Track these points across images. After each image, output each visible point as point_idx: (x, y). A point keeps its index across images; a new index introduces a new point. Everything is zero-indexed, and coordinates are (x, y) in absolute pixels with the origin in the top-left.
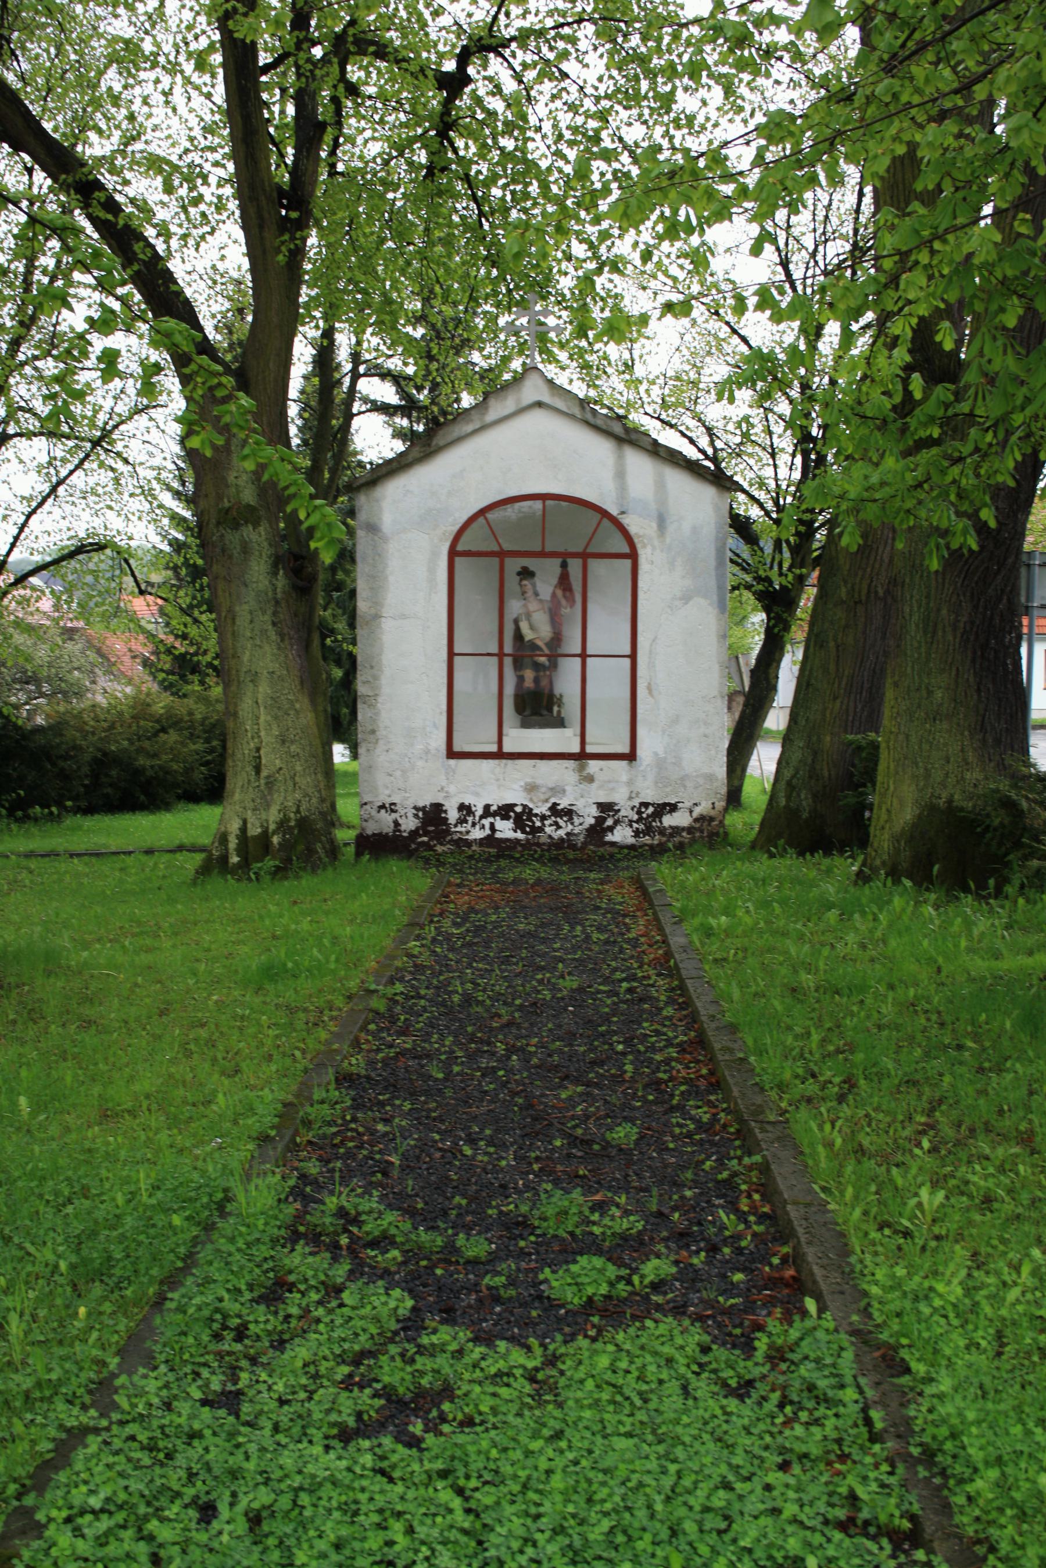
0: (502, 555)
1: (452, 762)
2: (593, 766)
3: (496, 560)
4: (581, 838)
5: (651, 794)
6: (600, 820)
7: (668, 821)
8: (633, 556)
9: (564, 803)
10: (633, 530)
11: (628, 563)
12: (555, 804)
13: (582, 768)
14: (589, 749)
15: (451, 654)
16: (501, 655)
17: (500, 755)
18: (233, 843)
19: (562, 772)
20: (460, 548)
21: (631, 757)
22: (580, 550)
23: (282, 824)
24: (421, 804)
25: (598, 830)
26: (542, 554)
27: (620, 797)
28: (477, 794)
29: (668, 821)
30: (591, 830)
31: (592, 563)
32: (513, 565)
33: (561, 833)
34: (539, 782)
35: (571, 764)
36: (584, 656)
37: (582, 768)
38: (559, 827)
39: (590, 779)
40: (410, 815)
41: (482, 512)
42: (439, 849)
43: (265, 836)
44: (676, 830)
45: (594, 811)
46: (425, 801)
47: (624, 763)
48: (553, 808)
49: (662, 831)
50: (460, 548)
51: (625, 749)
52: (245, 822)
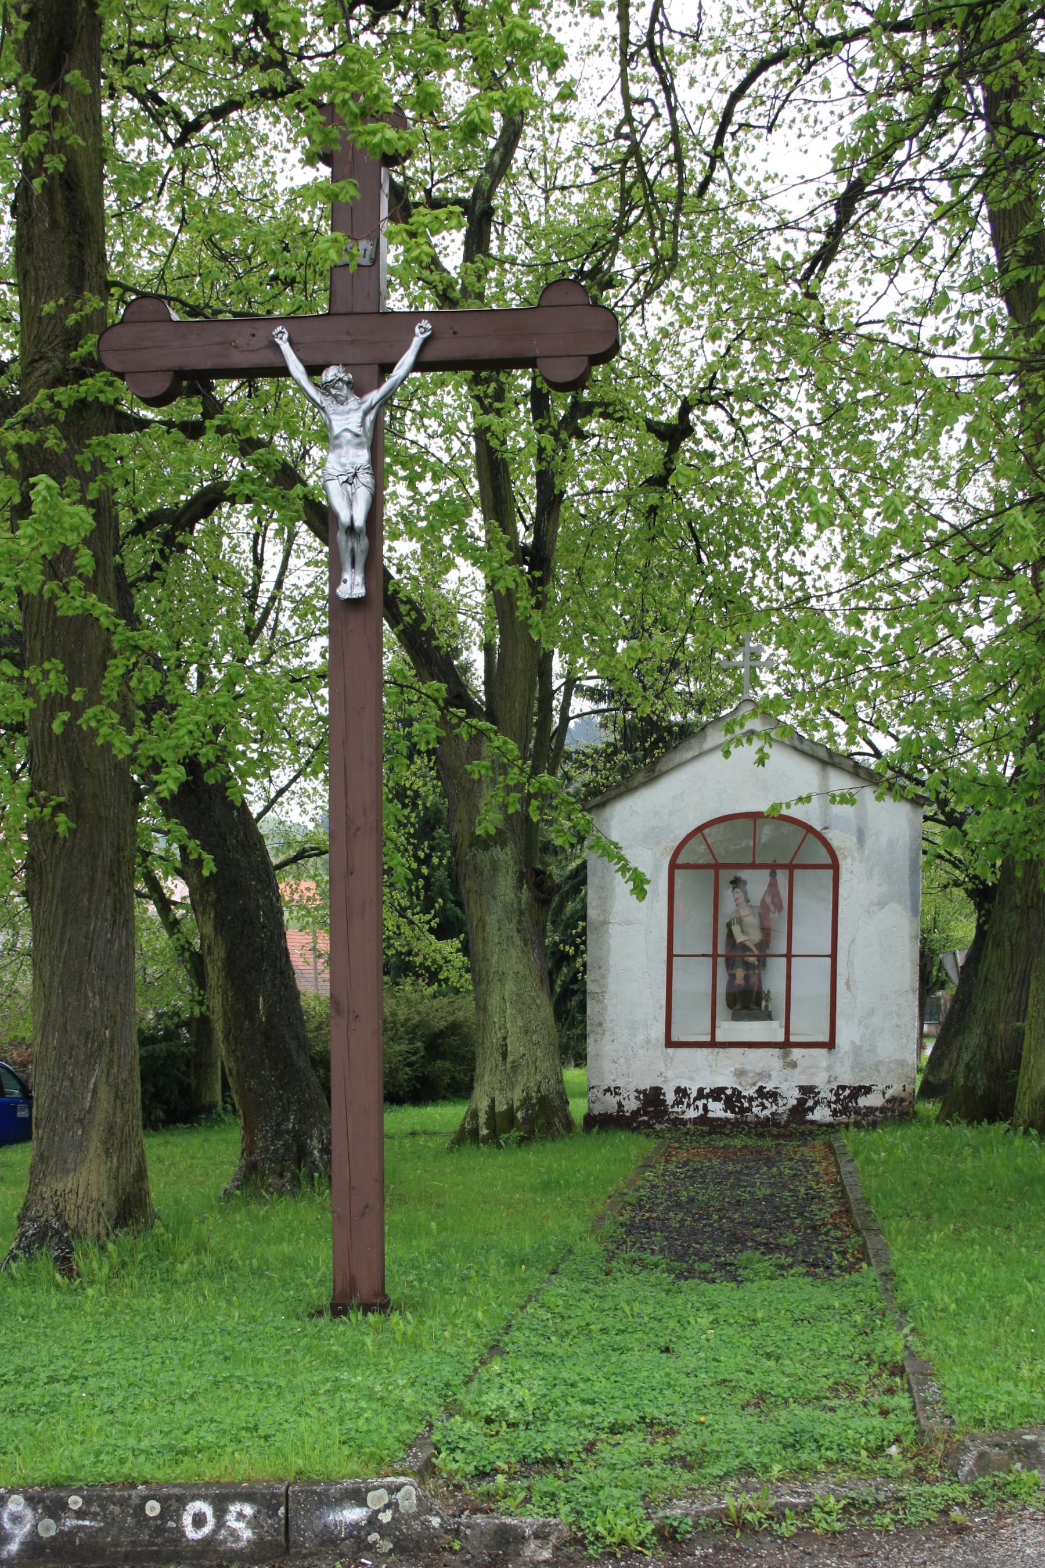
0: (717, 867)
1: (670, 1051)
2: (796, 1053)
3: (712, 872)
5: (848, 1078)
6: (801, 1102)
7: (863, 1102)
8: (834, 866)
9: (769, 1087)
10: (835, 843)
11: (830, 872)
12: (761, 1088)
13: (786, 1056)
14: (792, 1039)
15: (670, 956)
16: (715, 956)
17: (713, 1044)
18: (483, 1118)
19: (770, 1059)
20: (680, 861)
21: (830, 1045)
22: (787, 861)
23: (525, 1102)
24: (642, 1088)
25: (799, 1110)
26: (753, 866)
27: (820, 1081)
28: (692, 1079)
29: (863, 1102)
31: (796, 872)
32: (726, 875)
33: (767, 1113)
34: (748, 1067)
35: (776, 1051)
36: (789, 956)
37: (786, 1056)
38: (764, 1108)
39: (793, 1065)
41: (700, 829)
42: (658, 1127)
43: (510, 1112)
44: (871, 1110)
45: (797, 1094)
46: (646, 1085)
47: (824, 1051)
49: (857, 1111)
50: (680, 861)
51: (826, 1038)
52: (493, 1100)
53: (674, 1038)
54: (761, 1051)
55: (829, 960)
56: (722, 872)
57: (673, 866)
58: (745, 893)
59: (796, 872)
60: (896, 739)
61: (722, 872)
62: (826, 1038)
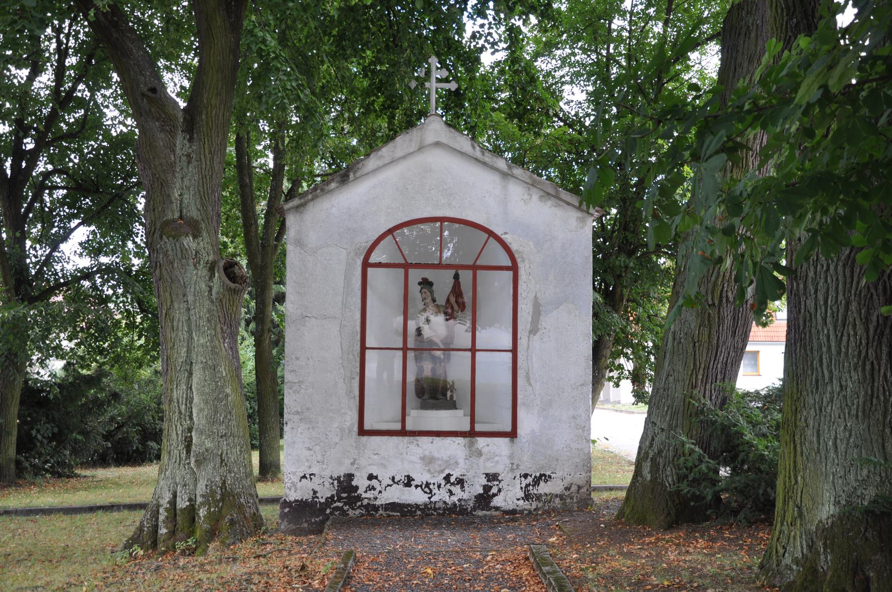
0: (406, 266)
1: (365, 439)
2: (481, 442)
3: (402, 271)
4: (471, 503)
6: (487, 488)
7: (543, 488)
8: (514, 268)
9: (456, 474)
10: (514, 247)
11: (510, 273)
13: (471, 445)
14: (478, 428)
15: (363, 348)
16: (405, 349)
17: (403, 432)
18: (163, 515)
19: (455, 447)
20: (373, 259)
21: (512, 434)
22: (471, 263)
23: (209, 497)
24: (335, 476)
25: (484, 499)
26: (440, 266)
28: (383, 466)
29: (543, 488)
30: (479, 498)
31: (479, 272)
32: (416, 276)
33: (455, 499)
34: (437, 455)
35: (460, 440)
36: (473, 350)
37: (471, 445)
38: (451, 493)
39: (480, 454)
40: (327, 484)
41: (390, 231)
42: (351, 513)
43: (192, 510)
45: (484, 481)
46: (341, 471)
47: (507, 440)
48: (447, 478)
49: (538, 497)
50: (373, 259)
52: (175, 496)
53: (367, 426)
54: (449, 440)
55: (510, 355)
56: (411, 271)
57: (366, 265)
58: (432, 292)
59: (479, 272)
60: (313, 498)
61: (411, 271)
62: (509, 429)
